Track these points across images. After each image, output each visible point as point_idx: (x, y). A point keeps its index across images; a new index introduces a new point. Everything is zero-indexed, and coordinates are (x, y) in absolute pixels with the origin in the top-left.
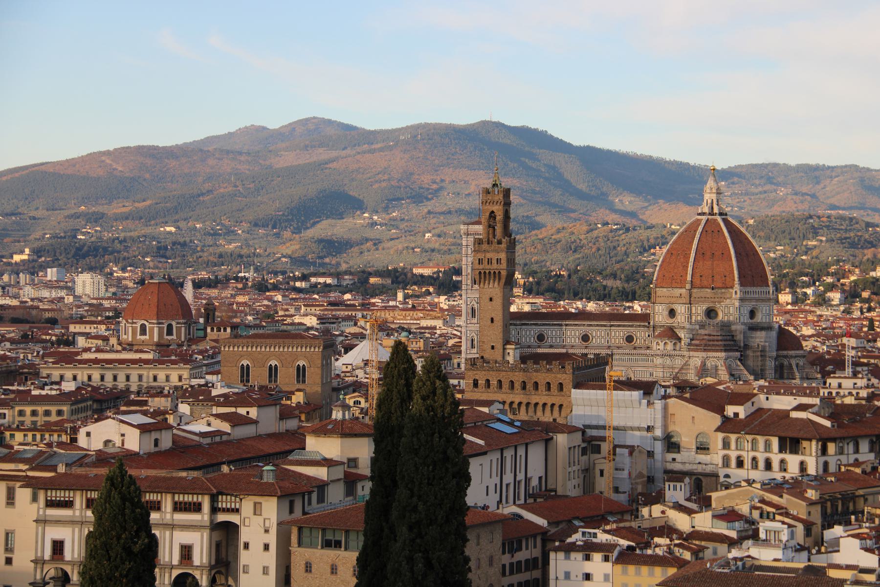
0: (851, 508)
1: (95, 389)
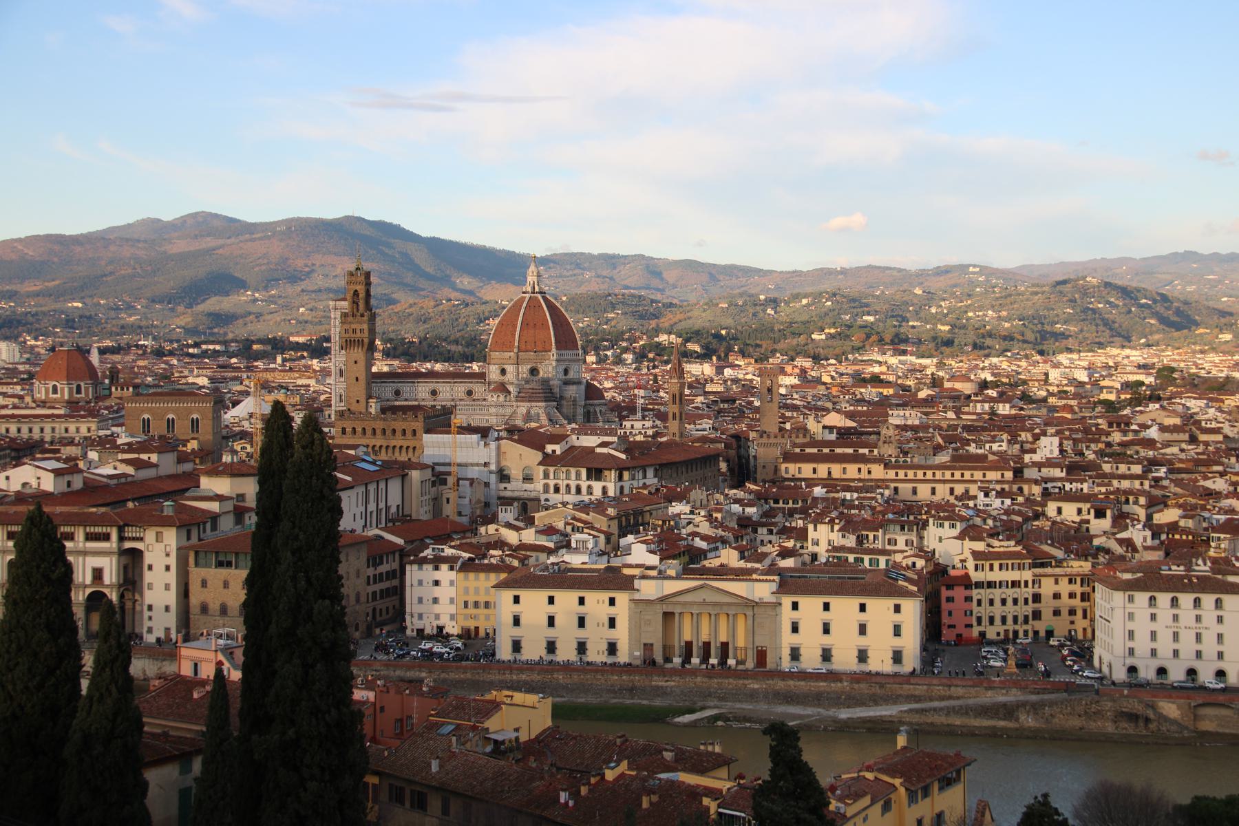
0: (640, 521)
1: (13, 440)
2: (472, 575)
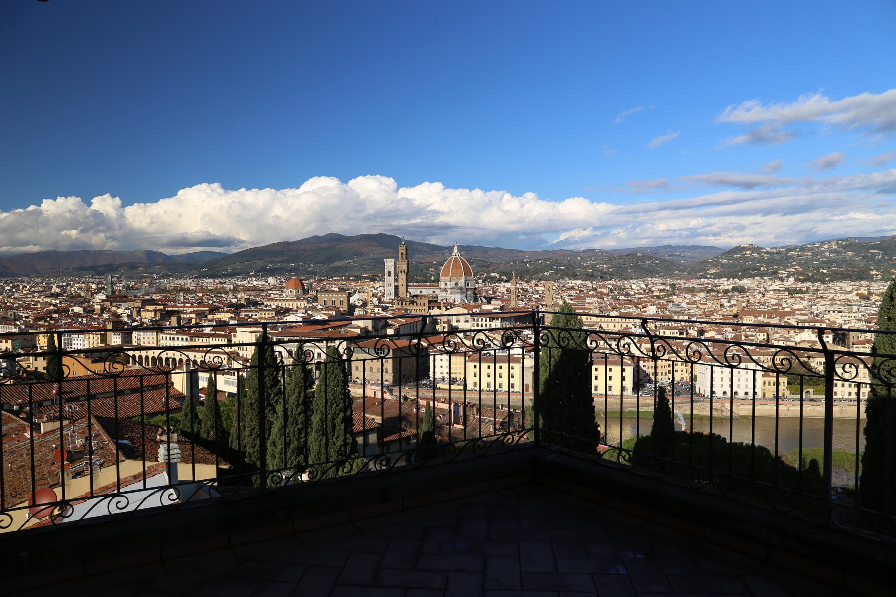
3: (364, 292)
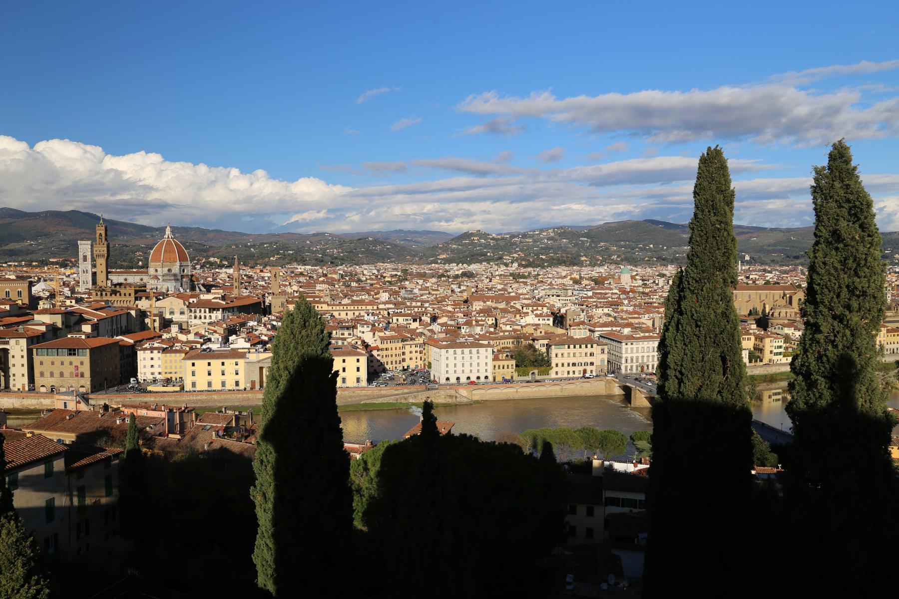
2: (168, 355)
3: (51, 280)
